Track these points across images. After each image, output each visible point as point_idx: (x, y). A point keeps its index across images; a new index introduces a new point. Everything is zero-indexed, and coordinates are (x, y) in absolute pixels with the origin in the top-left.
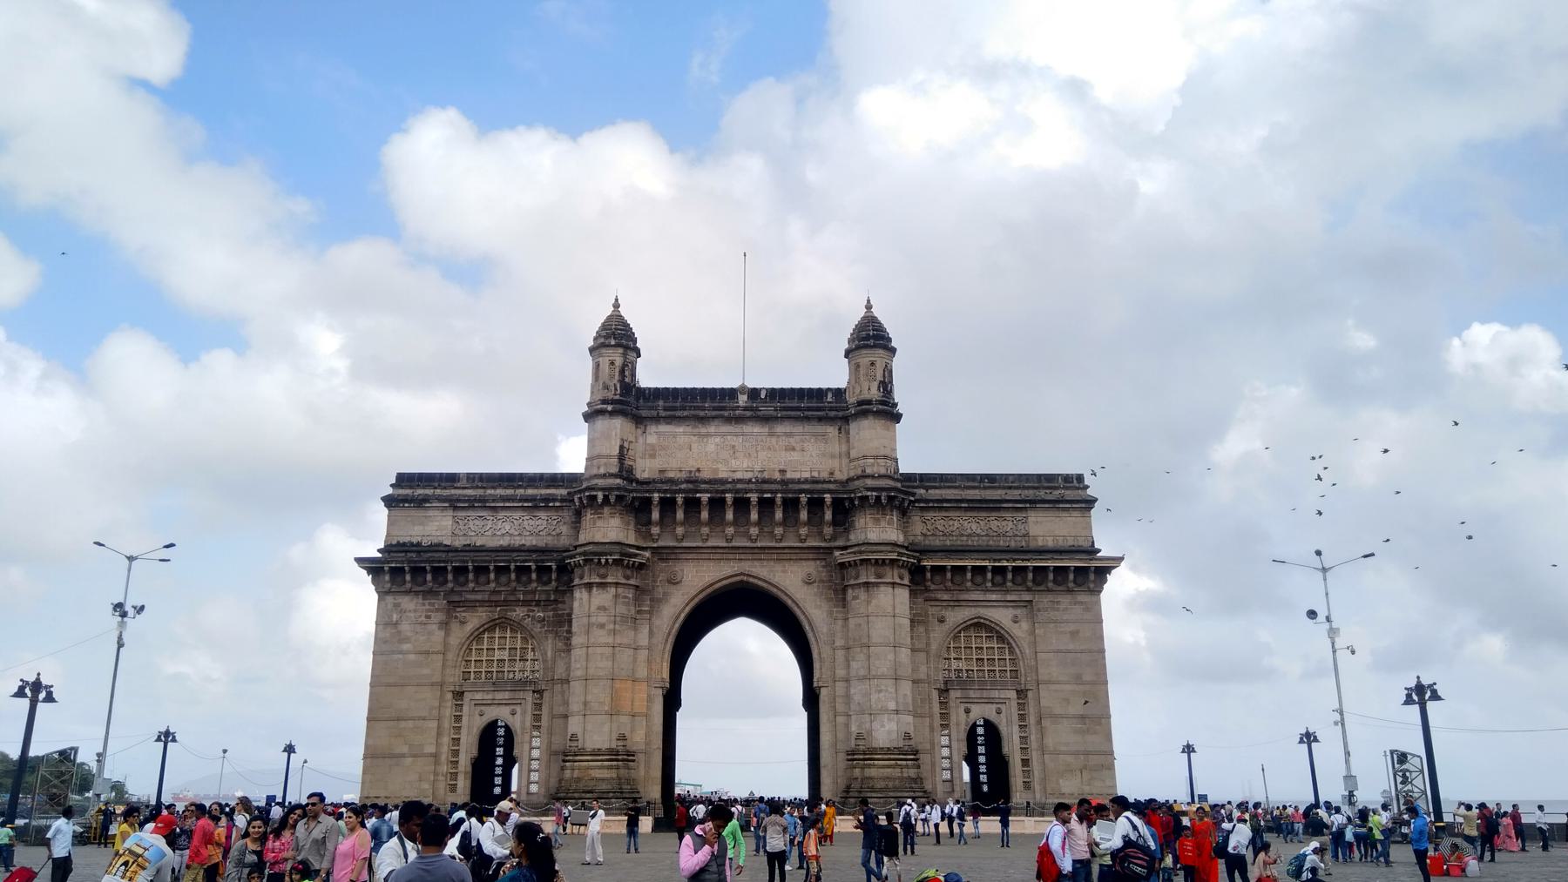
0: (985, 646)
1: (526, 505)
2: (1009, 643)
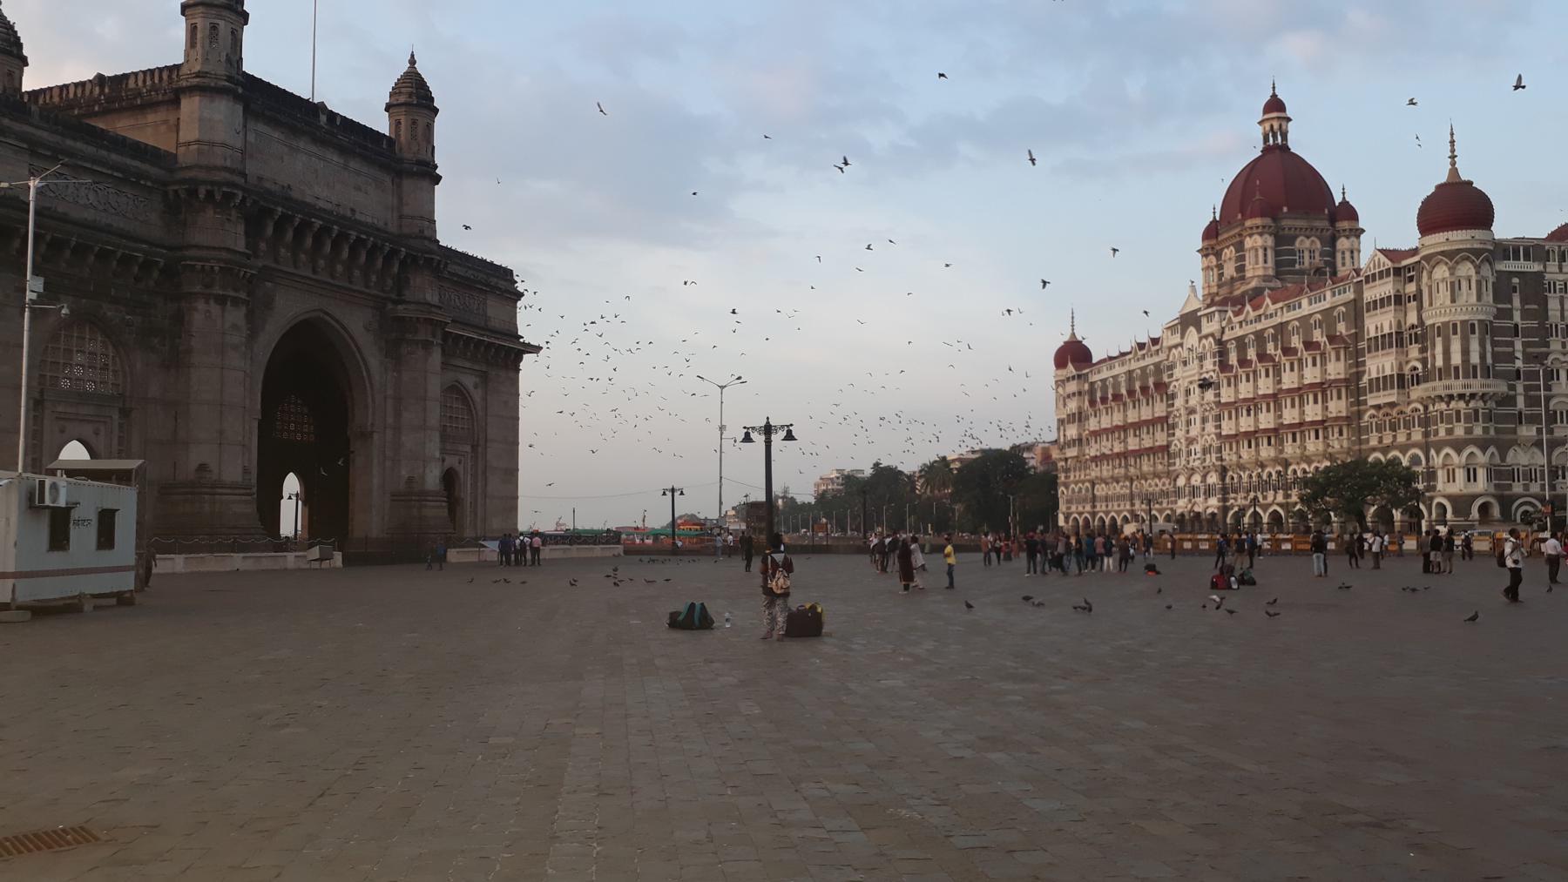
0: (454, 406)
1: (115, 174)
2: (470, 406)
